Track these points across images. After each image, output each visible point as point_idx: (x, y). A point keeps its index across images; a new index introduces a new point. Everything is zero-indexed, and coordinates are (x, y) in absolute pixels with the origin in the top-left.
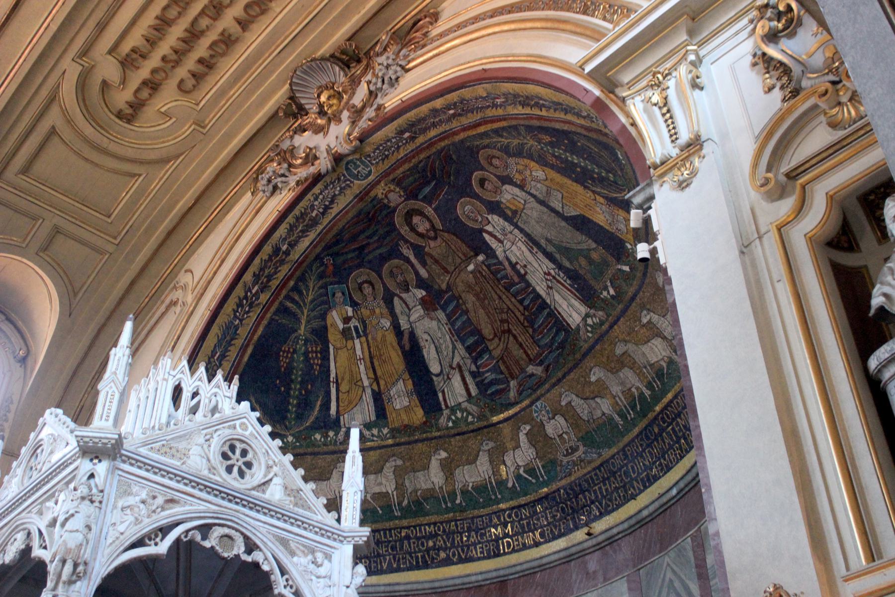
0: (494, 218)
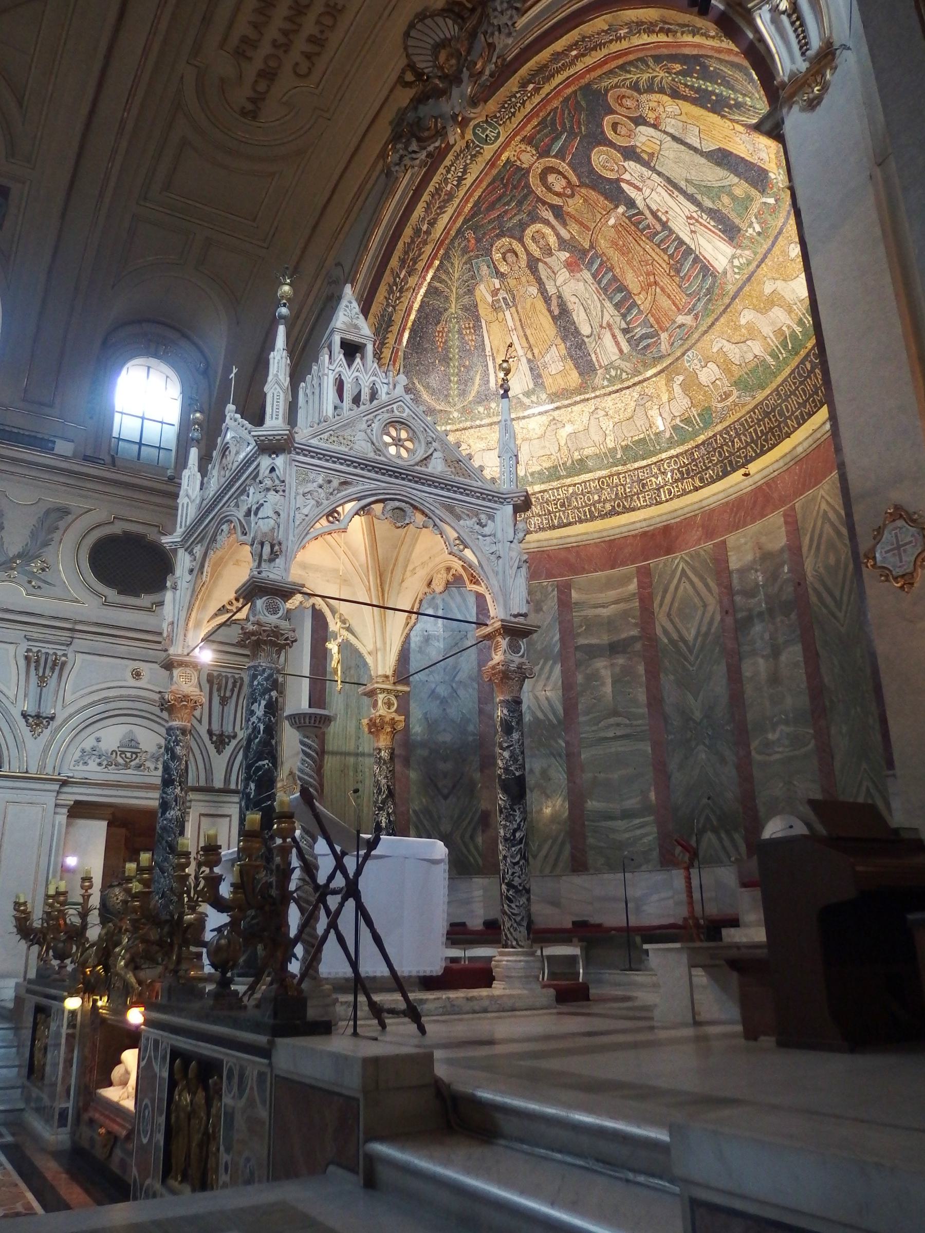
0: (631, 165)
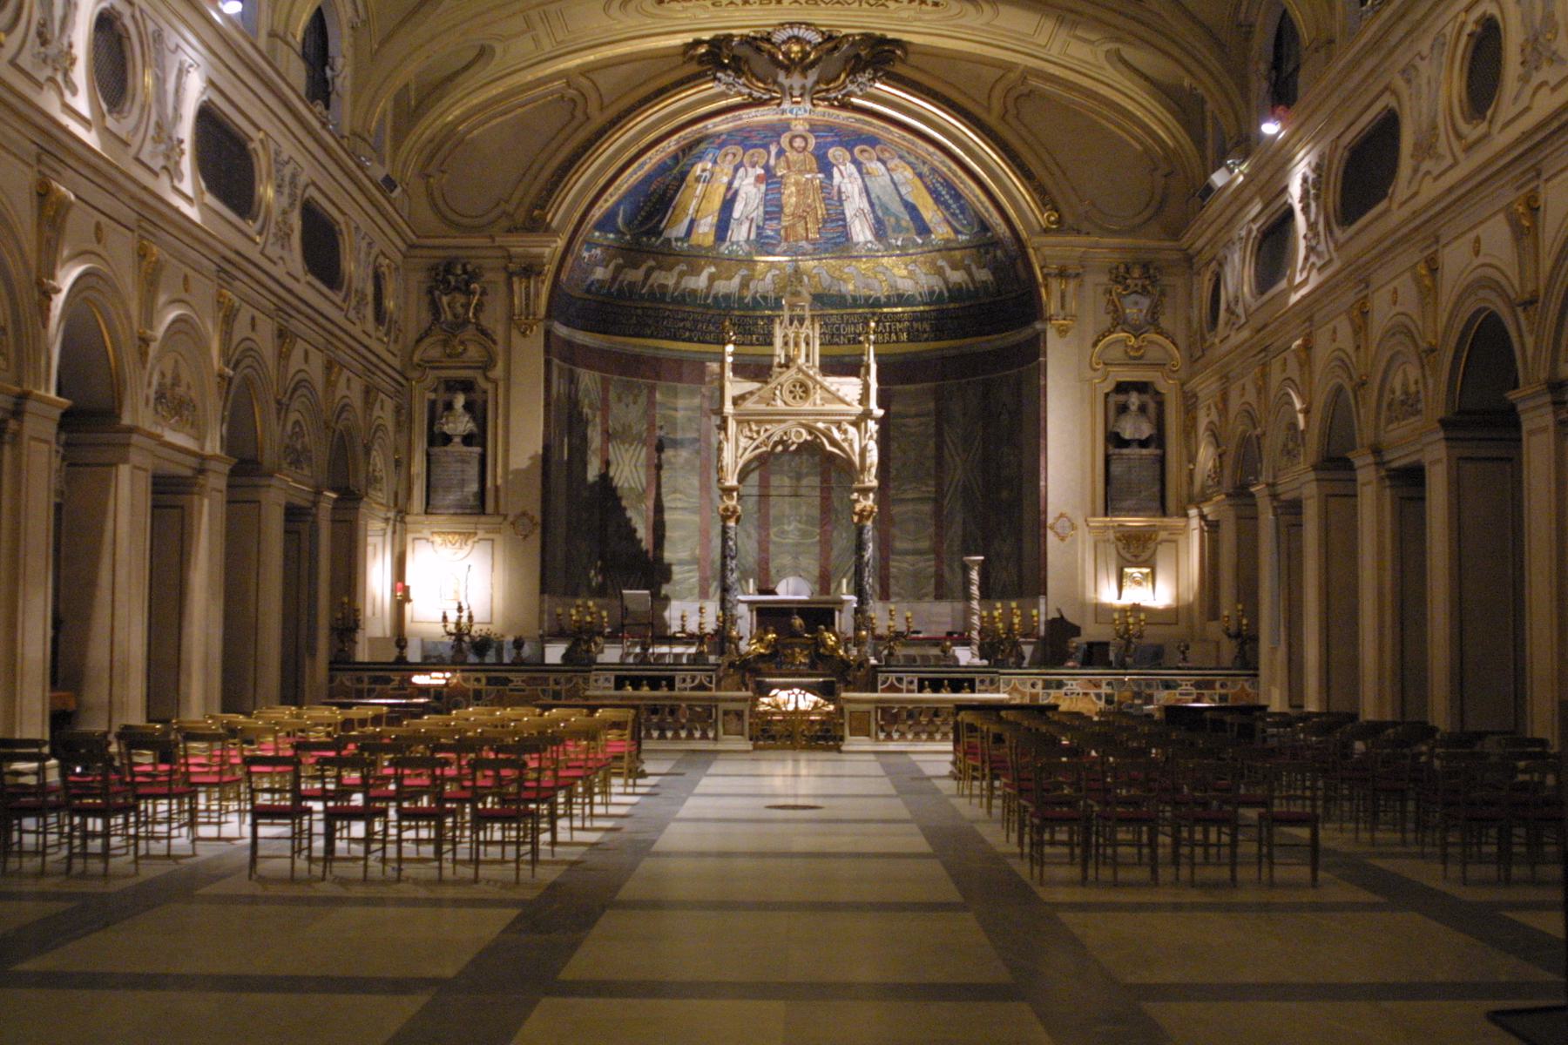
0: (852, 168)
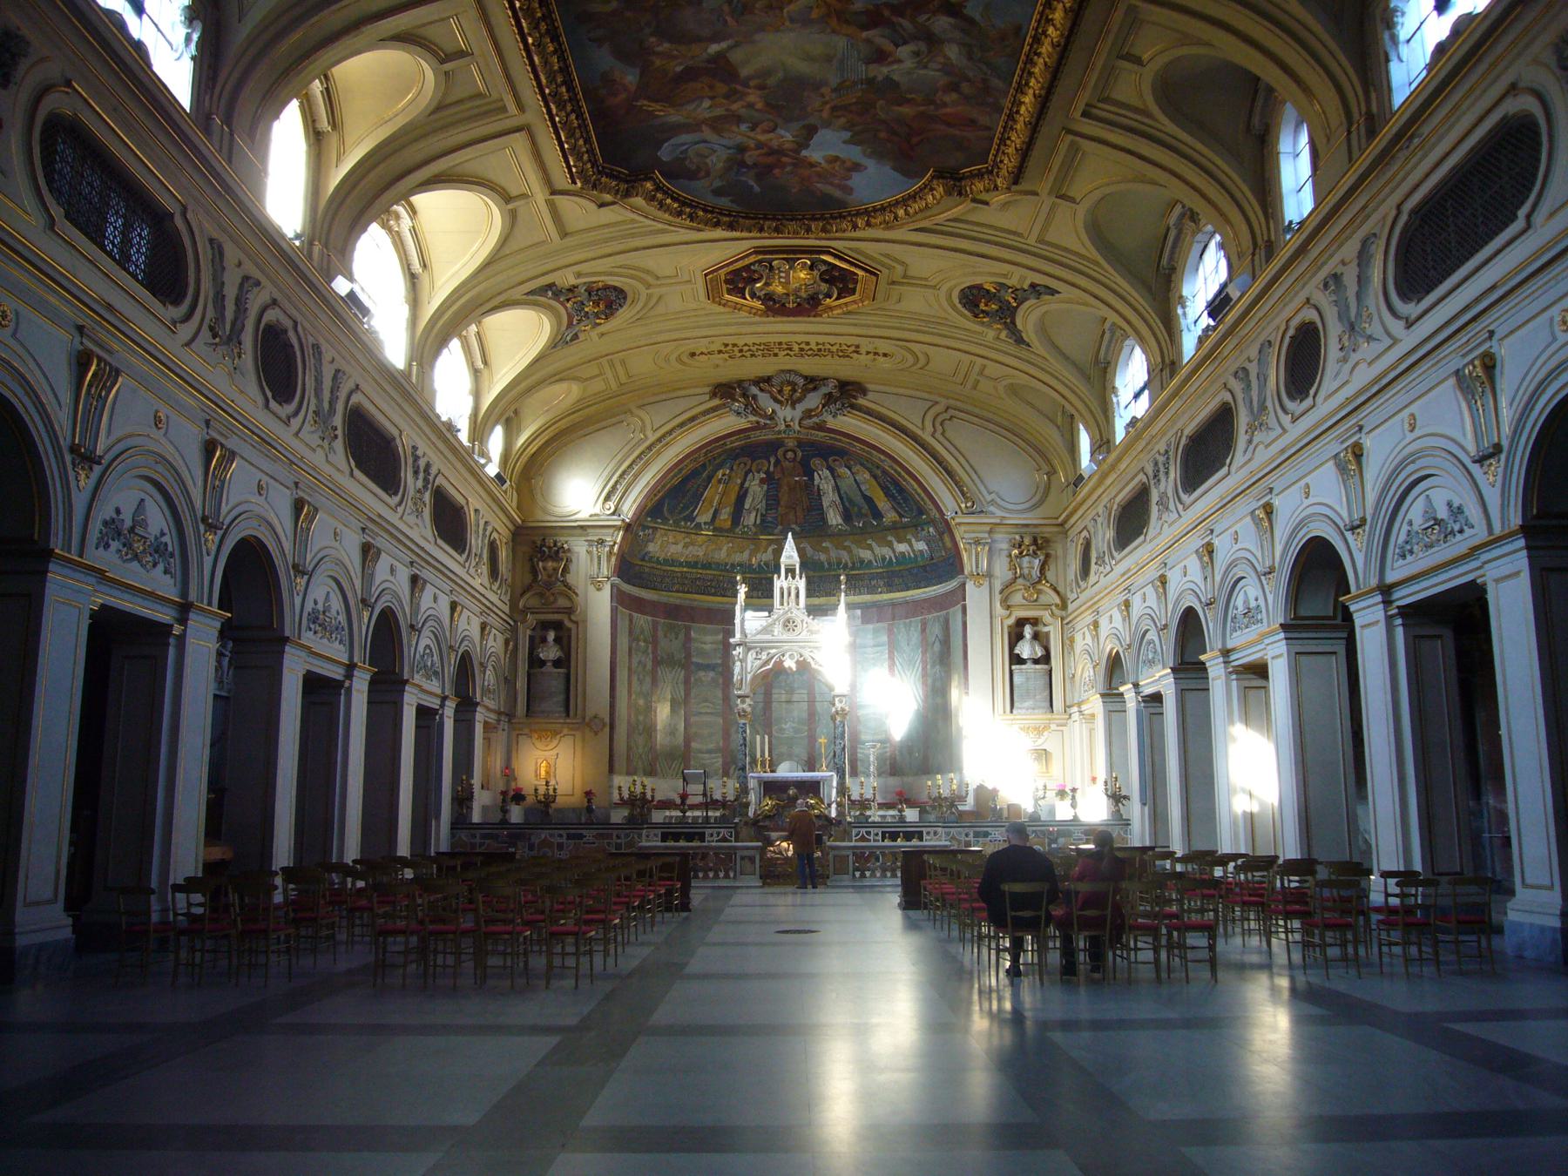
0: (827, 473)
